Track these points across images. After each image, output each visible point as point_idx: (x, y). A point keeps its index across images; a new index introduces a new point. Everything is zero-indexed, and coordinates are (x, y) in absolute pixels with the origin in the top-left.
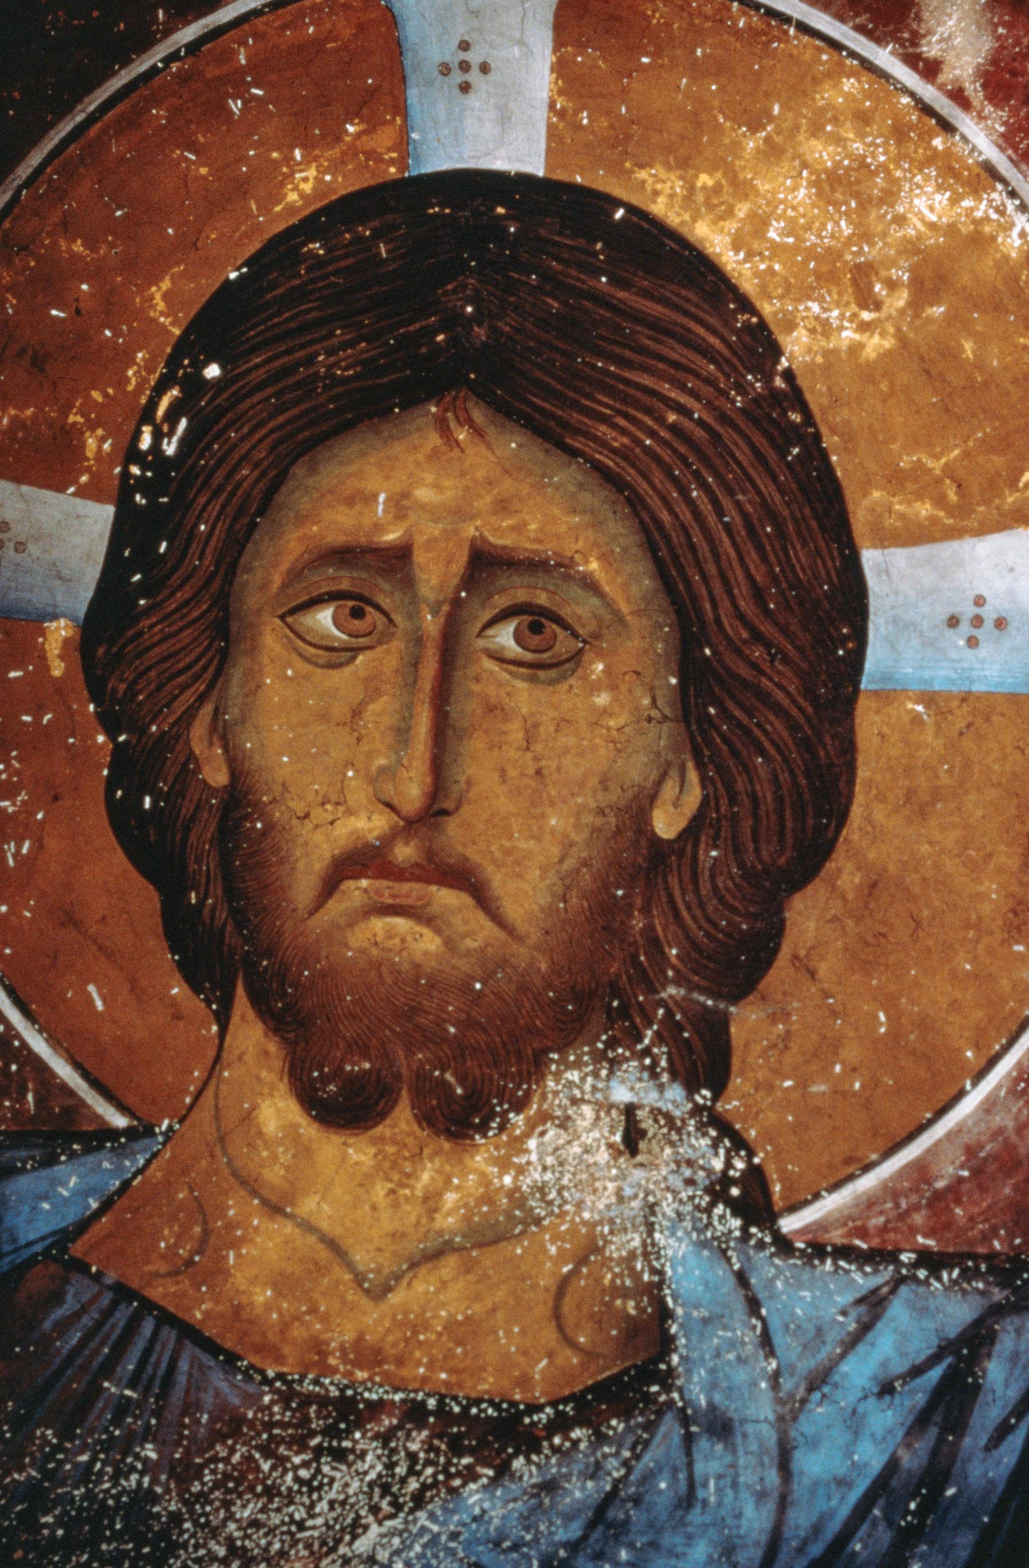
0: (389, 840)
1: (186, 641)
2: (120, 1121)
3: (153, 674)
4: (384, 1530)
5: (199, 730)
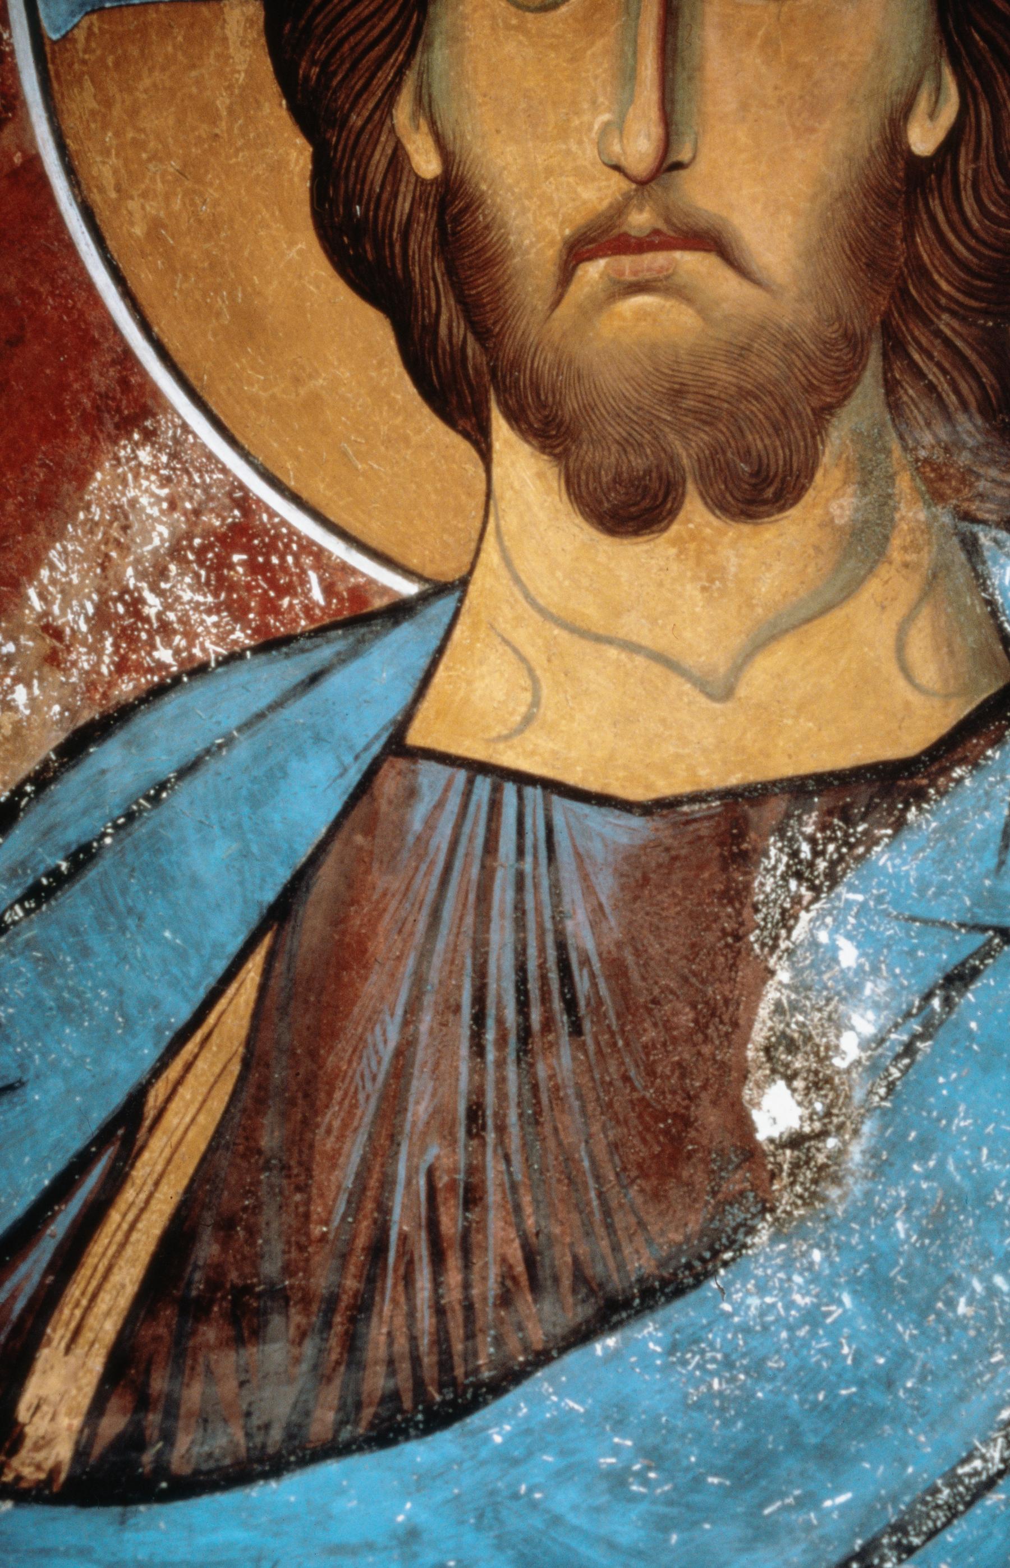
0: (620, 210)
2: (408, 588)
3: (346, 47)
4: (813, 914)
5: (403, 112)
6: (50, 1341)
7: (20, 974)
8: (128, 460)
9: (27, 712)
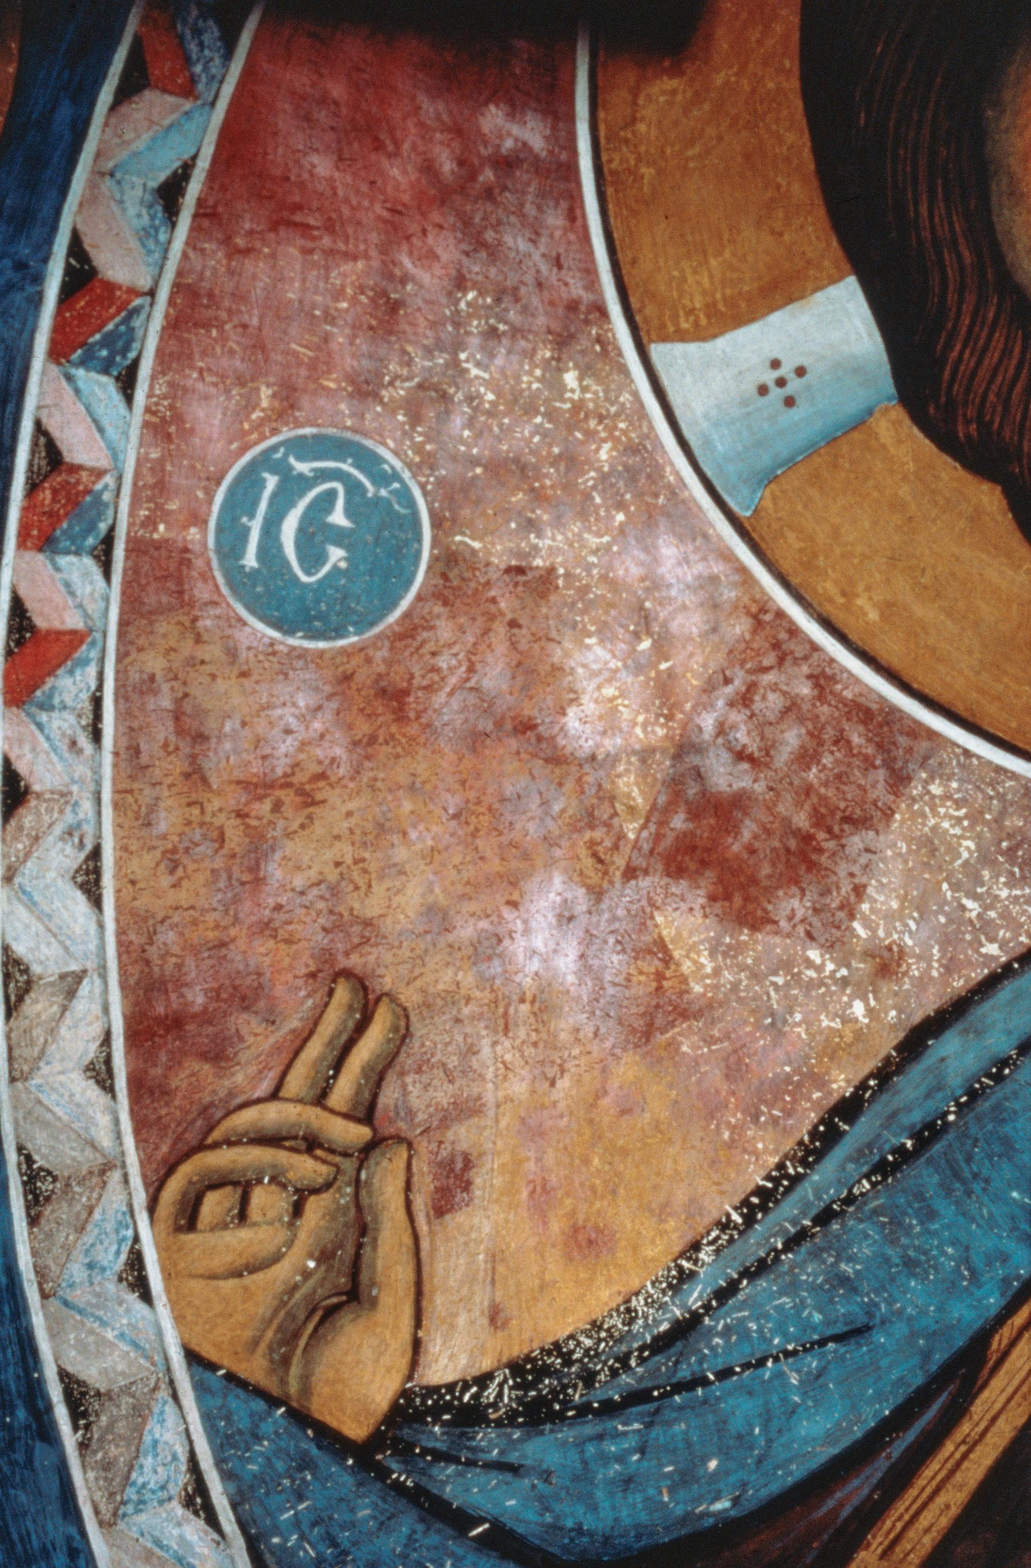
1: (1001, 346)
3: (992, 397)
6: (869, 1545)
7: (867, 1236)
8: (921, 797)
9: (866, 1021)
